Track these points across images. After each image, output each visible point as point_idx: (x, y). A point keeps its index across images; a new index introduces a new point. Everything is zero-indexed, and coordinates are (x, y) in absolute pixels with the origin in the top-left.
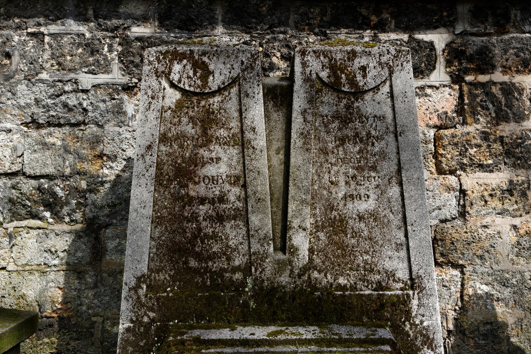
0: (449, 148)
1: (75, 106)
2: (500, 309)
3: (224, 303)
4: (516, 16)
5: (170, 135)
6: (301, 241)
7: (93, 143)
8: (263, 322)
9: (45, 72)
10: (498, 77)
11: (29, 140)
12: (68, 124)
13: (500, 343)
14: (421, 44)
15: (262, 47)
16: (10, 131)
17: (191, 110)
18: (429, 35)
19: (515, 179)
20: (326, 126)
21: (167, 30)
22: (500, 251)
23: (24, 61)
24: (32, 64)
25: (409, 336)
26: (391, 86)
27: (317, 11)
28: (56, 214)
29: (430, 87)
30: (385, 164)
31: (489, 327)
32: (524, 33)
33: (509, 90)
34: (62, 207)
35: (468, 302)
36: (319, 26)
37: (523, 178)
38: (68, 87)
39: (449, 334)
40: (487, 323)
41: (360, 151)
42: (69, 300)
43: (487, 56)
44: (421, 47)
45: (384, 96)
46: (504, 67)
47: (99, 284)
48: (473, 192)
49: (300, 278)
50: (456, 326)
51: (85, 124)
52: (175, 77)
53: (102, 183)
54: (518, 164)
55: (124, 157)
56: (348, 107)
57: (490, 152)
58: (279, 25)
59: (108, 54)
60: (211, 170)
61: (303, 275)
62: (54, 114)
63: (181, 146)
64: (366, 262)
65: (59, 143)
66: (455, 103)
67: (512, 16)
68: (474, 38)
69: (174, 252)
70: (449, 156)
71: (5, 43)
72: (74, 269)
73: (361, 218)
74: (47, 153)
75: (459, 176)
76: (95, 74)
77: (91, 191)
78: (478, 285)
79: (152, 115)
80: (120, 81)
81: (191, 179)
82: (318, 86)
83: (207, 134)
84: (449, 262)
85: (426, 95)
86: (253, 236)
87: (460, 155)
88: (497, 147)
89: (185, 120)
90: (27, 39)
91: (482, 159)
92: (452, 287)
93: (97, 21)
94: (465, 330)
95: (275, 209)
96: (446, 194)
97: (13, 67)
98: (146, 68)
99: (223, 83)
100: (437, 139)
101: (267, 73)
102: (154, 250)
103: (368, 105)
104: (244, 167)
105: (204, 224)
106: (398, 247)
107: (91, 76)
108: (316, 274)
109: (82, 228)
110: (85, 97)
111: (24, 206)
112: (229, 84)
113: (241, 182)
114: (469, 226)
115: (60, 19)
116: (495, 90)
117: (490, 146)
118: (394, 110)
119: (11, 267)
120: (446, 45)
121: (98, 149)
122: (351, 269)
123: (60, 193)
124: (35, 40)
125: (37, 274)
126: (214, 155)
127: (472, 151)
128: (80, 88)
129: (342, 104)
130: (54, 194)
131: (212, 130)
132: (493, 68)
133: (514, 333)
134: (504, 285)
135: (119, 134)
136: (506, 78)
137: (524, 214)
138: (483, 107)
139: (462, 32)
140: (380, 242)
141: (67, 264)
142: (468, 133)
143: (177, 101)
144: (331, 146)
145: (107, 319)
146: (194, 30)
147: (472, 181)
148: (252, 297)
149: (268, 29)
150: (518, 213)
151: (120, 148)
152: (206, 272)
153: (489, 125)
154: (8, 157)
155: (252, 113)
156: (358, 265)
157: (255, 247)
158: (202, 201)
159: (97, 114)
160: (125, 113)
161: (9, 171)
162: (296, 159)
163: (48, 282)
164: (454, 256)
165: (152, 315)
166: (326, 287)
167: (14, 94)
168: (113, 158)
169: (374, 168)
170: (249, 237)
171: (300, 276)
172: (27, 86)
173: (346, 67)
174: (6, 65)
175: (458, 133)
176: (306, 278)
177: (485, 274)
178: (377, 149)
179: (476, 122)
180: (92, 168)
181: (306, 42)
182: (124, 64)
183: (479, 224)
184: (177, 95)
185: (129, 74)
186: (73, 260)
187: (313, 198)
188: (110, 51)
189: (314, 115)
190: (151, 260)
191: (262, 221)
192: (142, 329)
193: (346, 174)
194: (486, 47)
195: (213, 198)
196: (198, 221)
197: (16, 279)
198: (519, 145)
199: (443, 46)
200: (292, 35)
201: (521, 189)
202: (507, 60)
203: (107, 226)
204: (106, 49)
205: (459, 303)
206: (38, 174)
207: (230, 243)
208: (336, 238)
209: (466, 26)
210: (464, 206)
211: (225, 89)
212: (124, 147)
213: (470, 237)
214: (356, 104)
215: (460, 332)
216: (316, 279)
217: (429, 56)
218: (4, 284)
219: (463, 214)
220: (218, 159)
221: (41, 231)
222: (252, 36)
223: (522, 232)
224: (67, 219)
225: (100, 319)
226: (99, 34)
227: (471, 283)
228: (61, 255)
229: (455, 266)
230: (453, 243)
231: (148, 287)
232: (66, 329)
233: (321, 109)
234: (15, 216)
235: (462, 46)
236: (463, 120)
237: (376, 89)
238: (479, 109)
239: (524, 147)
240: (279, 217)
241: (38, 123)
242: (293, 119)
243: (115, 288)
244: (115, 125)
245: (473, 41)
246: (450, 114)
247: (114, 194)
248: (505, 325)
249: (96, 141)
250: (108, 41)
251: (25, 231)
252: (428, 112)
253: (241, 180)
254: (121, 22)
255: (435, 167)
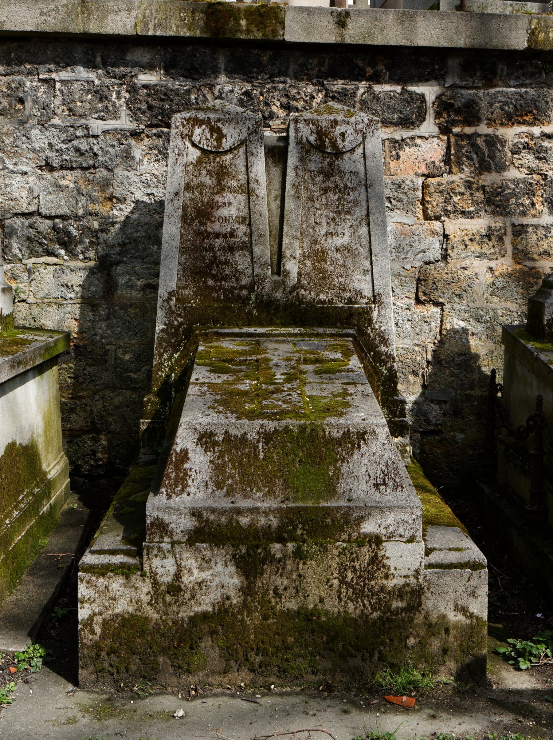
0: (435, 196)
1: (86, 151)
2: (473, 342)
3: (234, 312)
4: (502, 70)
5: (192, 184)
6: (292, 267)
7: (104, 186)
8: (262, 325)
9: (57, 118)
10: (483, 129)
11: (45, 182)
12: (79, 168)
13: (472, 372)
14: (413, 96)
15: (263, 96)
16: (26, 173)
17: (209, 165)
18: (421, 88)
19: (493, 225)
20: (313, 179)
21: (173, 78)
22: (477, 290)
23: (37, 106)
24: (44, 109)
25: (370, 337)
26: (364, 149)
27: (315, 62)
28: (71, 252)
29: (420, 137)
30: (357, 210)
31: (463, 358)
32: (510, 87)
33: (493, 142)
34: (76, 246)
35: (445, 336)
36: (317, 77)
37: (501, 225)
38: (79, 133)
39: (428, 365)
40: (462, 354)
41: (339, 199)
42: (84, 330)
43: (474, 108)
44: (413, 99)
45: (358, 156)
46: (489, 119)
47: (111, 316)
48: (455, 237)
49: (290, 294)
50: (434, 357)
51: (94, 167)
52: (196, 139)
53: (113, 224)
54: (497, 212)
55: (133, 199)
56: (330, 165)
57: (472, 200)
58: (279, 75)
59: (116, 101)
60: (224, 212)
61: (293, 292)
62: (67, 158)
63: (201, 193)
64: (340, 283)
65: (72, 186)
66: (442, 153)
67: (499, 71)
68: (463, 92)
69: (196, 274)
70: (434, 203)
71: (17, 88)
72: (88, 302)
73: (338, 250)
74: (61, 195)
75: (443, 222)
76: (105, 120)
77: (102, 231)
78: (455, 321)
79: (179, 169)
80: (128, 127)
81: (208, 219)
82: (307, 147)
83: (221, 184)
84: (431, 300)
85: (416, 145)
86: (256, 262)
87: (445, 202)
88: (479, 195)
89: (204, 172)
90: (39, 84)
91: (465, 206)
92: (433, 323)
93: (106, 68)
94: (442, 360)
95: (273, 243)
96: (431, 238)
97: (27, 113)
98: (173, 131)
99: (234, 145)
100: (425, 186)
101: (267, 122)
102: (181, 272)
103: (345, 163)
104: (250, 209)
105: (219, 253)
106: (365, 272)
107: (100, 122)
108: (303, 292)
109: (95, 265)
110: (95, 142)
111: (40, 244)
112: (238, 145)
113: (247, 222)
114: (449, 268)
115: (70, 66)
116: (480, 141)
117: (473, 194)
118: (365, 167)
119: (31, 300)
120: (436, 98)
121: (108, 191)
122: (329, 288)
123: (74, 233)
124: (46, 85)
125: (55, 306)
126: (226, 200)
127: (456, 199)
128: (91, 133)
129: (326, 162)
130: (68, 234)
131: (225, 181)
132: (479, 120)
133: (485, 363)
134: (479, 321)
135: (128, 178)
136: (490, 131)
137: (500, 257)
138: (467, 157)
139: (451, 86)
140: (352, 269)
141: (82, 297)
142: (453, 182)
143: (197, 157)
144: (316, 194)
145: (119, 348)
146: (198, 79)
147: (455, 226)
148: (255, 307)
149: (269, 78)
150: (495, 257)
151: (129, 191)
152: (220, 289)
153: (472, 175)
154: (24, 198)
155: (256, 168)
156: (335, 286)
157: (258, 271)
158: (217, 235)
159: (107, 158)
160: (133, 158)
161: (27, 211)
162: (289, 204)
163: (65, 314)
164: (435, 295)
165: (180, 319)
166: (310, 301)
167: (28, 138)
168: (122, 200)
169: (349, 212)
170: (252, 263)
171: (290, 292)
172: (40, 131)
173: (329, 133)
174: (19, 110)
175: (444, 182)
176: (295, 294)
177: (462, 311)
178: (351, 198)
179: (460, 172)
180: (103, 209)
181: (304, 92)
182: (131, 110)
183: (458, 266)
184: (198, 153)
185: (137, 120)
186: (87, 294)
187: (302, 235)
188: (119, 97)
189: (305, 170)
190: (179, 279)
191: (263, 250)
192: (173, 330)
193: (327, 216)
194: (473, 101)
195: (226, 234)
196: (214, 251)
197: (35, 311)
198: (499, 194)
199: (433, 98)
200: (291, 85)
201: (498, 235)
202: (492, 113)
203: (118, 263)
204: (114, 96)
205: (438, 337)
206: (53, 215)
207: (239, 268)
208: (318, 265)
209: (456, 80)
210: (446, 250)
211: (235, 148)
212: (133, 190)
213: (450, 277)
214: (337, 162)
215: (438, 362)
216: (303, 295)
217: (419, 108)
218: (25, 315)
219: (445, 257)
220: (230, 204)
221: (58, 267)
222: (252, 86)
223: (497, 273)
224: (81, 257)
225: (113, 348)
226: (108, 81)
227: (449, 319)
228: (77, 289)
229: (437, 304)
230: (434, 283)
231: (176, 300)
232: (82, 356)
233: (309, 166)
234: (33, 253)
235: (451, 99)
236: (450, 169)
237: (353, 150)
238: (465, 159)
239: (503, 196)
240: (276, 249)
241: (52, 167)
242: (287, 173)
243: (126, 320)
244: (123, 170)
245: (462, 94)
246: (437, 163)
247: (124, 234)
248: (477, 357)
249: (105, 184)
250: (116, 88)
251: (42, 267)
252: (417, 161)
253: (247, 221)
254: (129, 69)
255: (422, 213)
